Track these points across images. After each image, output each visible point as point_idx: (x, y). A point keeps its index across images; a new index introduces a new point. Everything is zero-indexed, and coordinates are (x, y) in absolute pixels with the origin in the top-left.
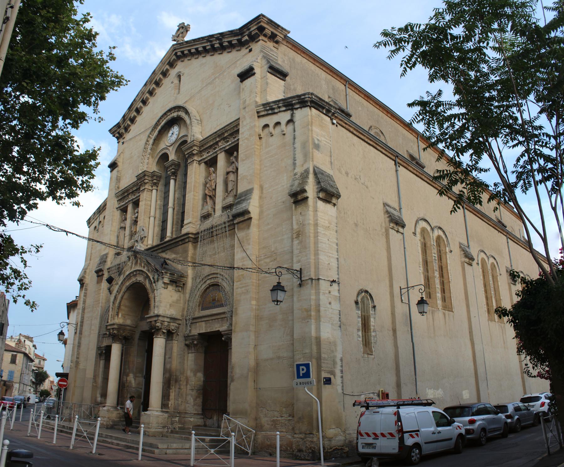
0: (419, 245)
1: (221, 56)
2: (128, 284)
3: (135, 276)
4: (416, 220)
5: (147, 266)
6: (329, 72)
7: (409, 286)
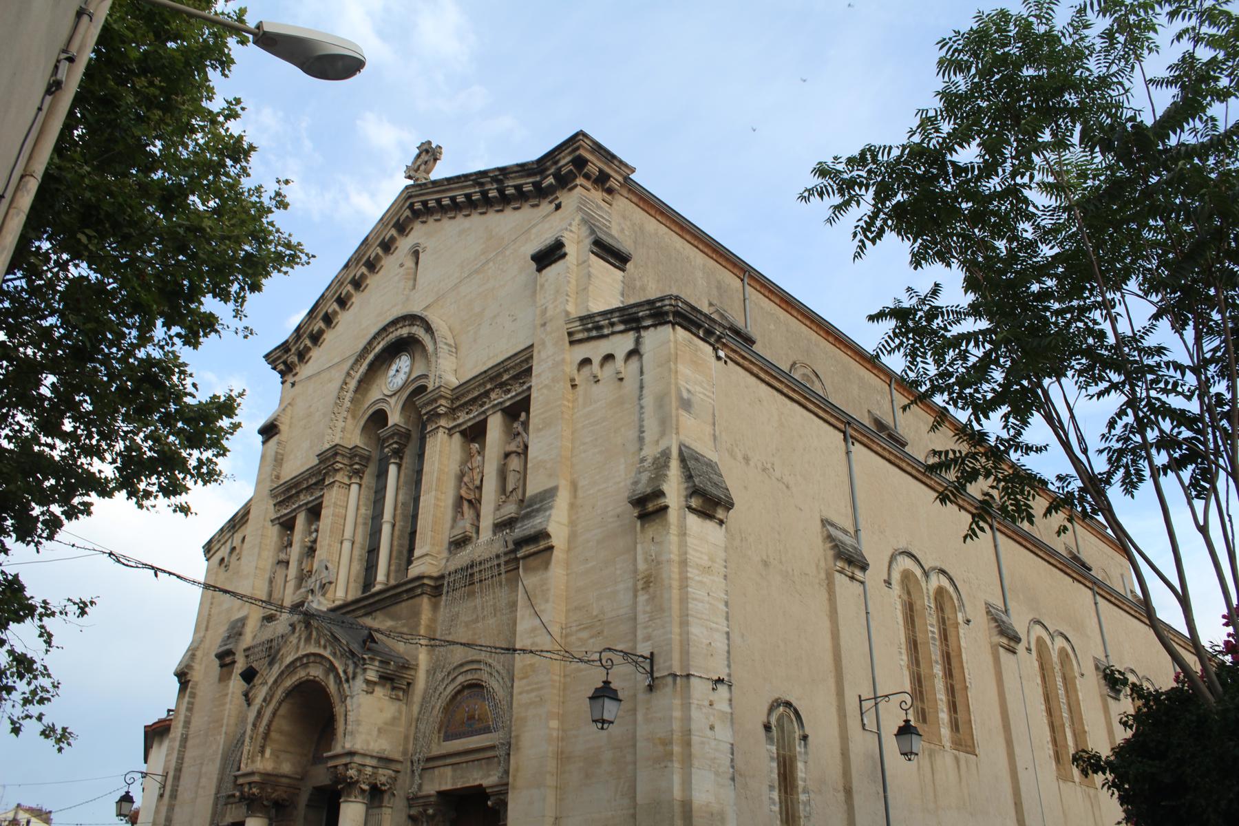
0: (899, 607)
1: (499, 215)
2: (288, 683)
3: (305, 666)
4: (890, 554)
5: (331, 644)
6: (710, 253)
7: (879, 694)
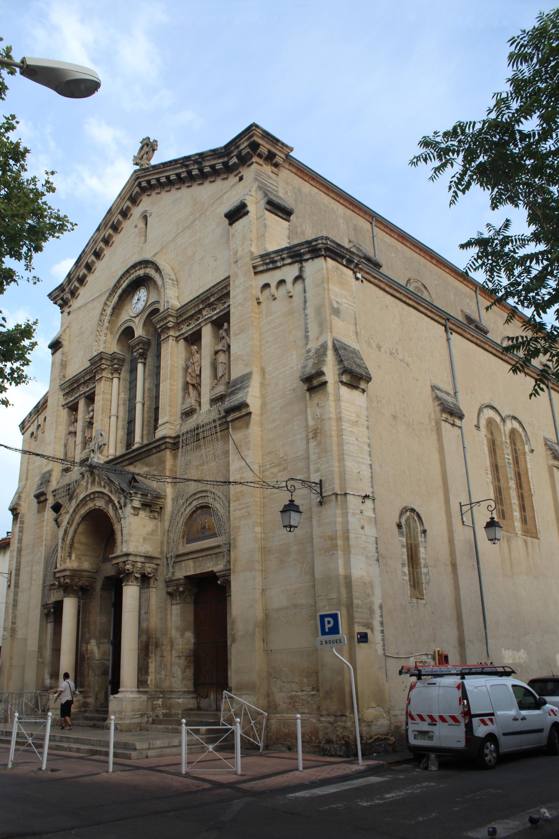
0: (485, 443)
1: (201, 187)
2: (83, 511)
3: (93, 500)
4: (478, 407)
5: (108, 485)
6: (348, 205)
7: (473, 501)
